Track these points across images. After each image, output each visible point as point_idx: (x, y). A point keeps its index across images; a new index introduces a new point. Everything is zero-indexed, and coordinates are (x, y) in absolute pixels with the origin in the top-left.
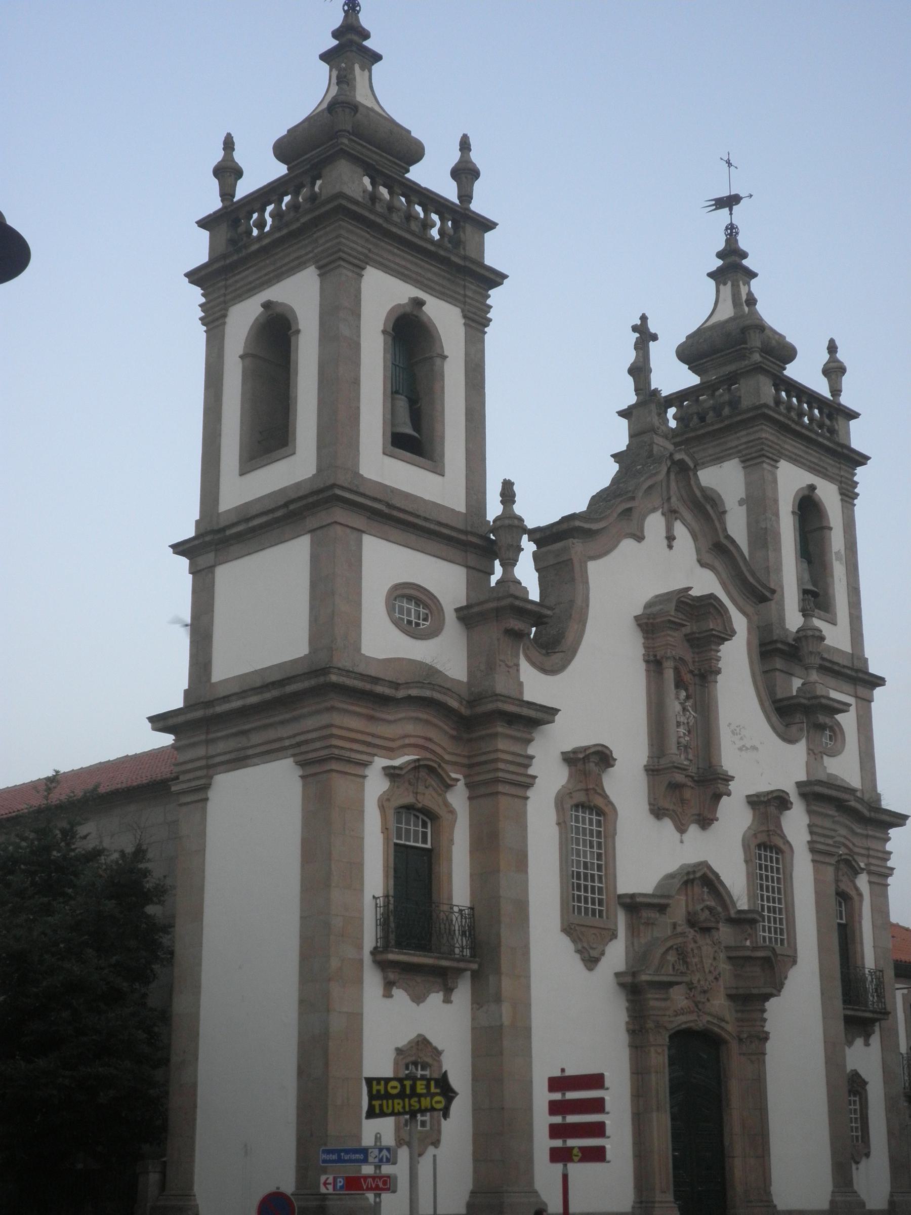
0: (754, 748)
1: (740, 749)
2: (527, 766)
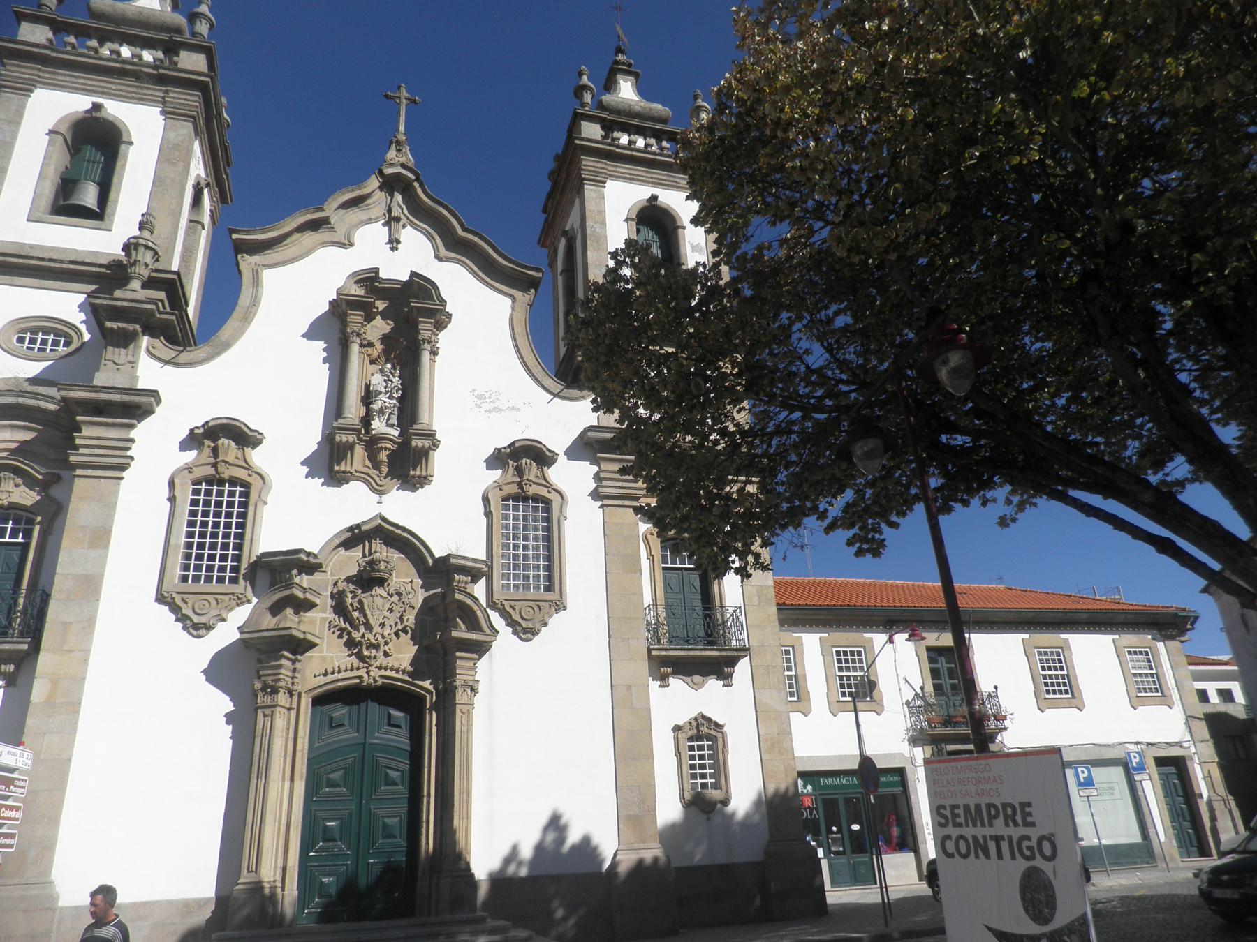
0: (513, 408)
1: (489, 411)
2: (128, 449)
